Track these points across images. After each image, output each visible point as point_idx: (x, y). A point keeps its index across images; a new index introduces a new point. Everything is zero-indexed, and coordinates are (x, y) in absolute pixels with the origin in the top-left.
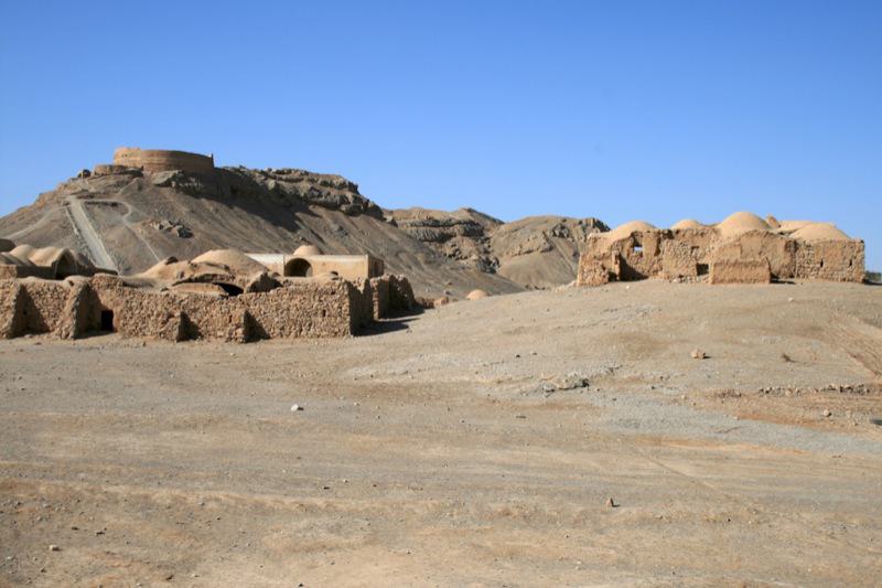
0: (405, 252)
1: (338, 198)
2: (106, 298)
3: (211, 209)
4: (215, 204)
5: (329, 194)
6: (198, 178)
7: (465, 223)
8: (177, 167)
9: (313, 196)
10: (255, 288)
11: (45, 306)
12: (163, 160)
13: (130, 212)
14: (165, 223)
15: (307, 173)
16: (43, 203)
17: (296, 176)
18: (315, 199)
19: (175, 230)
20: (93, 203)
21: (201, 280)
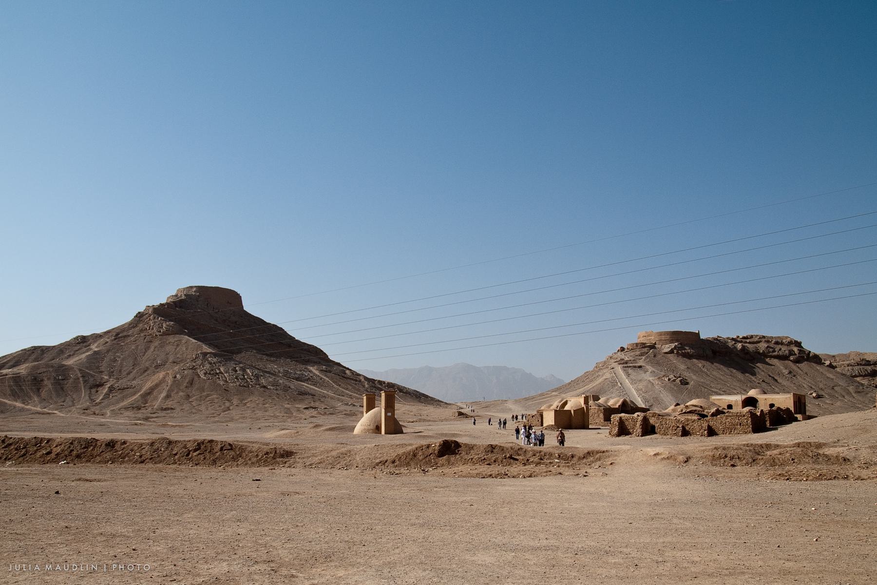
2: (652, 421)
3: (700, 365)
6: (691, 347)
8: (677, 341)
10: (713, 415)
11: (629, 425)
15: (764, 337)
16: (599, 368)
17: (756, 339)
19: (678, 380)
21: (690, 412)
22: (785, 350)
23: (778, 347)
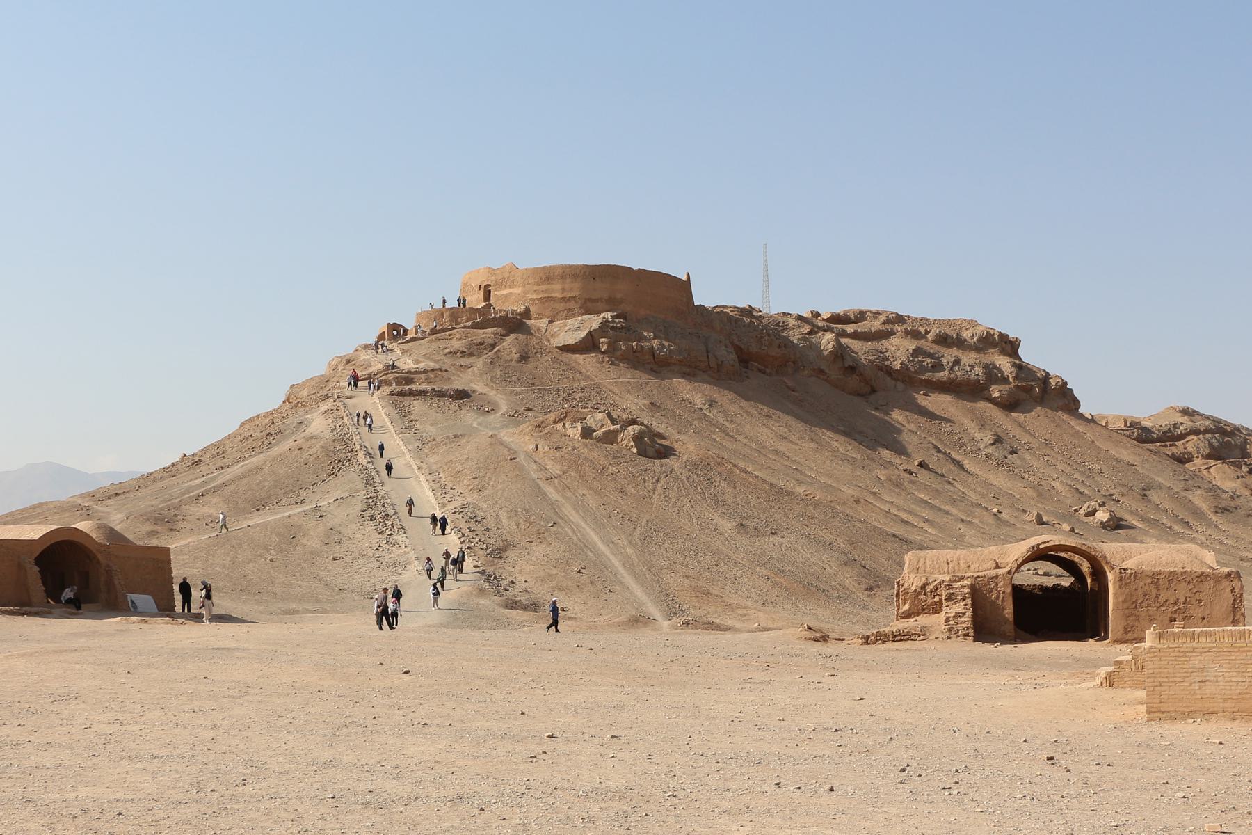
0: (1160, 486)
1: (979, 370)
3: (698, 400)
4: (706, 387)
5: (957, 362)
7: (1206, 431)
8: (611, 303)
9: (923, 370)
12: (574, 289)
13: (504, 408)
14: (596, 419)
15: (900, 319)
17: (876, 325)
18: (927, 375)
20: (411, 393)
22: (971, 364)
23: (949, 355)
